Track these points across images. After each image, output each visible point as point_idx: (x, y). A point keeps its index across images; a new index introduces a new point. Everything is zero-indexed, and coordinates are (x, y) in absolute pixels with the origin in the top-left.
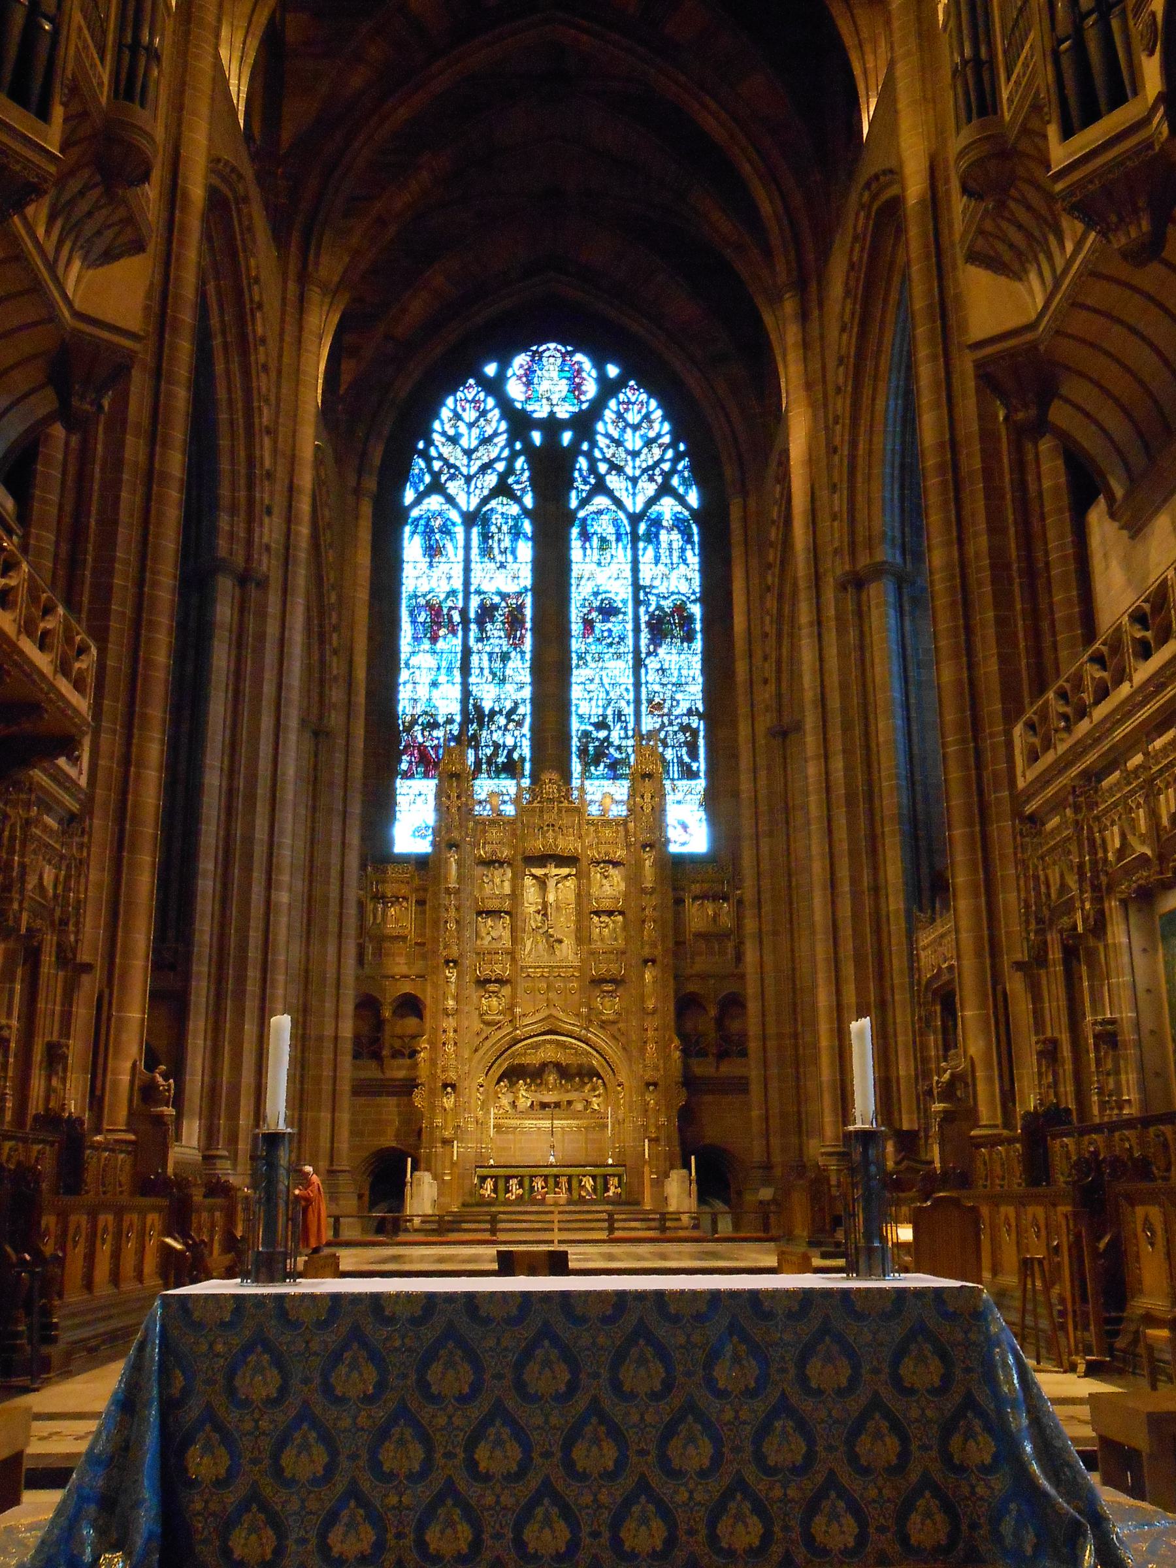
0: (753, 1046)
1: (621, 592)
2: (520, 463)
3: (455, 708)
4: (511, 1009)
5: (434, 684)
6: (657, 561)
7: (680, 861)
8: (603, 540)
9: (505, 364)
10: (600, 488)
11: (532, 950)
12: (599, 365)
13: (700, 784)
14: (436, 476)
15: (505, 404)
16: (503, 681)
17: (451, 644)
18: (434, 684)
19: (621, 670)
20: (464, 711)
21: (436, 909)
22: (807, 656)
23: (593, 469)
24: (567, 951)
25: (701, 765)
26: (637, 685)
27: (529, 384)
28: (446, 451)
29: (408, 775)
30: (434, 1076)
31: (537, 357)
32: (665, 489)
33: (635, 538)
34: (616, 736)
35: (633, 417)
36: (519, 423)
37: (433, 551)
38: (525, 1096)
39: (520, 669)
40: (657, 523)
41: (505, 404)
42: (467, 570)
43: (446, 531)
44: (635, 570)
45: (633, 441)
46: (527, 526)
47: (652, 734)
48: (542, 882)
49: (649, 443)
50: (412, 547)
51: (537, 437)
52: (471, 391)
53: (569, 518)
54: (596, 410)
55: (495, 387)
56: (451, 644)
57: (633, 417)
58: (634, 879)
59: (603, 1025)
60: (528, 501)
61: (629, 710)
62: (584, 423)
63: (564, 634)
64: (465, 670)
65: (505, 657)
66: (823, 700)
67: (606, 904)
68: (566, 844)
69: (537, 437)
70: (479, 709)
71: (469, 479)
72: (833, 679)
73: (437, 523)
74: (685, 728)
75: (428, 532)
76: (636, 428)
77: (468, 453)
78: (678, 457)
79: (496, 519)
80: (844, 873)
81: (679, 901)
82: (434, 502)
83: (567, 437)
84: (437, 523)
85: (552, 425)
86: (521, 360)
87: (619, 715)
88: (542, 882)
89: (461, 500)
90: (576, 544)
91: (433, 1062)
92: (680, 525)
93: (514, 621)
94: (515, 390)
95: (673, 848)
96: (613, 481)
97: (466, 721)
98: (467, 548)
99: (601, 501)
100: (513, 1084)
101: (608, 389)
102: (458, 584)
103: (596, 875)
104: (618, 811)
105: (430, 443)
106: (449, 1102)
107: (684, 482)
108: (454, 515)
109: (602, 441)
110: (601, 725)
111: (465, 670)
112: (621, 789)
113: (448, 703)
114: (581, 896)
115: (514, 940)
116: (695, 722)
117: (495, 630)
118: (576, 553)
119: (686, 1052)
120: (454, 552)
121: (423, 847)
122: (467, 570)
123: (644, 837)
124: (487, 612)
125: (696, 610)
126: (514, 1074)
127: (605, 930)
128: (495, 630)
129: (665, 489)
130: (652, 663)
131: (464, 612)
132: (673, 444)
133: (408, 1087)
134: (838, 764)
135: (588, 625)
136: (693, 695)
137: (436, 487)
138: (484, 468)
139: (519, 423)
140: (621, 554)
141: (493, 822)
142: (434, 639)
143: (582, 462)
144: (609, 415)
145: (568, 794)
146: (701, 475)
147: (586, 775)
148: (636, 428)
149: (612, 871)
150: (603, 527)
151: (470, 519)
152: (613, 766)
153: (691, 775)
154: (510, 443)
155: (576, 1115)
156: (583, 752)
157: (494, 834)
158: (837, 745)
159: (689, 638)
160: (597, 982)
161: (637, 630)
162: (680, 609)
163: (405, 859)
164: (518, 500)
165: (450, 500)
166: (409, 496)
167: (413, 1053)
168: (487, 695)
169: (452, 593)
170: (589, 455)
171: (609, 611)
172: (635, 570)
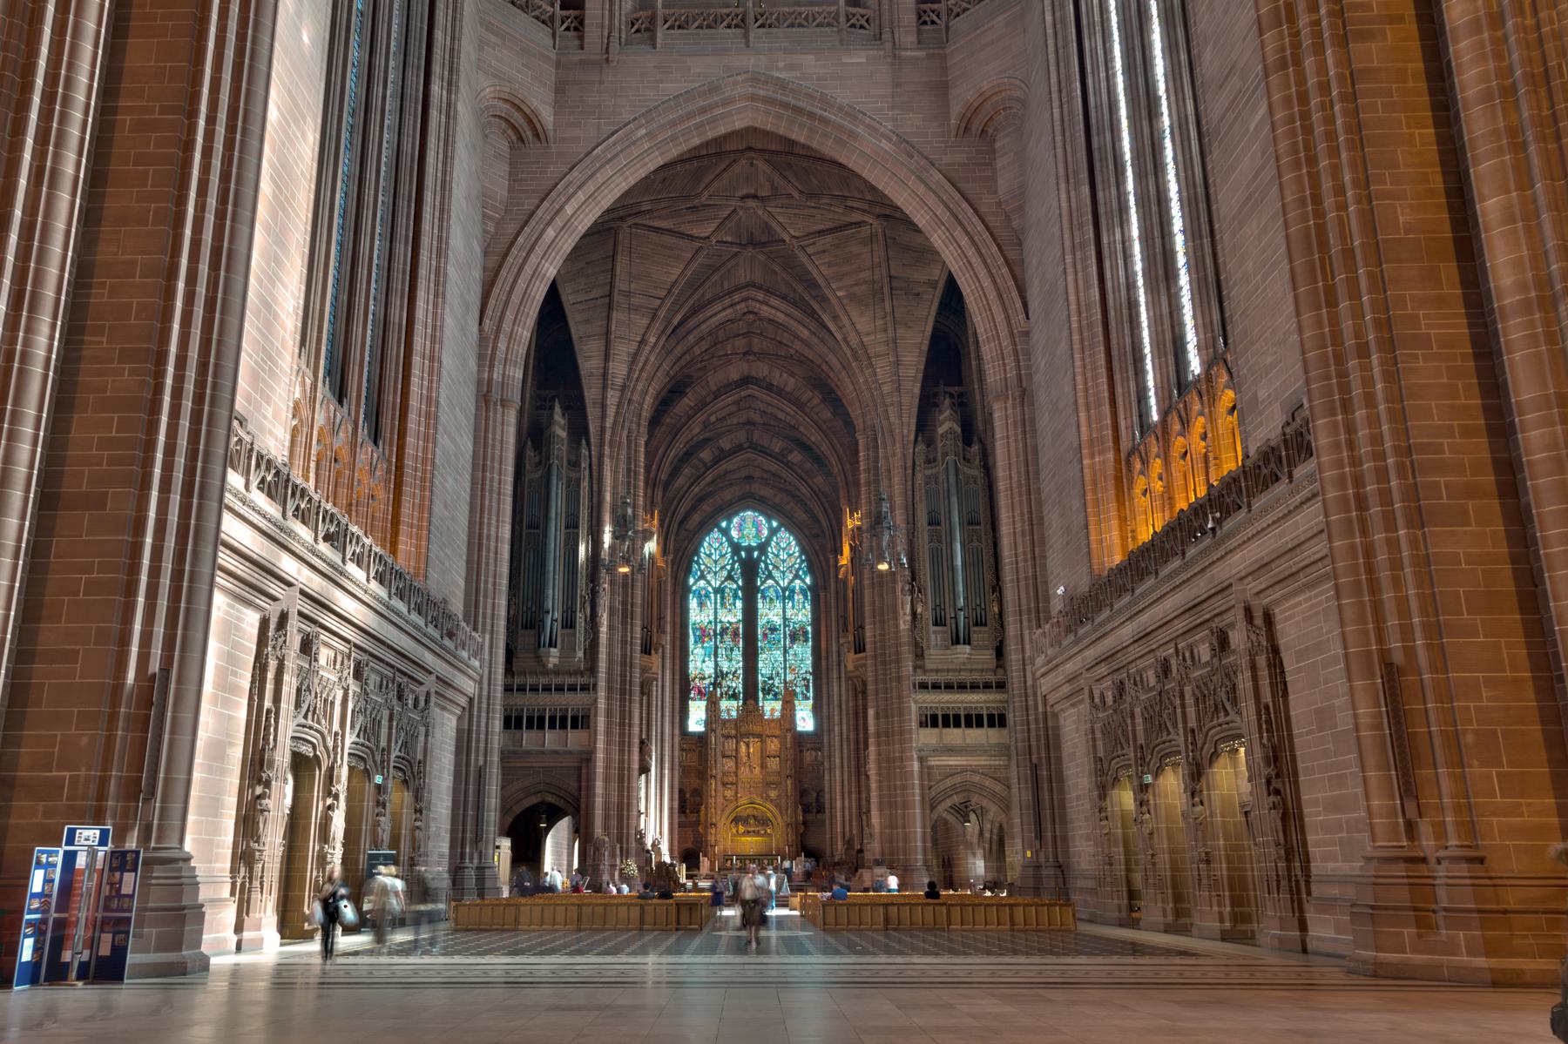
0: (827, 811)
1: (778, 621)
2: (737, 565)
3: (712, 671)
4: (736, 793)
5: (704, 661)
6: (793, 607)
7: (802, 735)
8: (771, 599)
9: (730, 522)
10: (770, 576)
11: (744, 772)
12: (769, 520)
13: (811, 702)
14: (702, 572)
15: (730, 539)
16: (731, 660)
17: (709, 644)
18: (704, 661)
19: (778, 654)
20: (716, 673)
21: (706, 755)
22: (836, 689)
23: (767, 568)
24: (757, 770)
25: (811, 694)
26: (785, 661)
27: (740, 530)
28: (706, 561)
29: (693, 699)
30: (706, 821)
31: (743, 520)
32: (797, 576)
33: (784, 598)
34: (777, 681)
35: (783, 545)
36: (736, 548)
37: (701, 605)
38: (741, 829)
39: (738, 655)
40: (793, 591)
41: (730, 539)
42: (716, 613)
43: (707, 596)
44: (784, 612)
45: (783, 556)
46: (740, 593)
47: (791, 682)
48: (748, 746)
49: (790, 556)
50: (693, 603)
51: (743, 554)
52: (716, 534)
53: (757, 589)
54: (769, 540)
55: (726, 532)
56: (709, 644)
57: (783, 545)
58: (783, 743)
59: (771, 801)
60: (740, 583)
61: (782, 671)
62: (762, 548)
63: (755, 639)
64: (716, 655)
65: (732, 650)
66: (840, 706)
67: (773, 753)
68: (757, 729)
69: (743, 554)
70: (721, 672)
71: (715, 573)
72: (844, 698)
73: (703, 592)
74: (804, 679)
75: (700, 596)
76: (784, 549)
77: (715, 562)
78: (802, 562)
79: (727, 590)
80: (845, 764)
81: (801, 751)
82: (702, 583)
83: (756, 554)
84: (703, 592)
85: (749, 549)
86: (736, 520)
87: (778, 674)
88: (748, 746)
89: (713, 583)
90: (760, 601)
91: (706, 815)
92: (803, 592)
93: (735, 634)
94: (734, 534)
95: (799, 729)
96: (776, 574)
97: (717, 677)
98: (716, 603)
99: (770, 582)
100: (737, 824)
101: (773, 532)
102: (712, 618)
103: (768, 741)
104: (777, 714)
105: (699, 557)
106: (713, 831)
107: (804, 573)
108: (710, 589)
109: (771, 556)
110: (771, 678)
111: (716, 655)
112: (778, 705)
113: (709, 669)
114: (763, 750)
115: (737, 767)
116: (810, 677)
117: (727, 638)
118: (760, 605)
119: (804, 811)
120: (710, 605)
121: (701, 729)
122: (716, 613)
123: (787, 726)
124: (724, 631)
125: (809, 628)
126: (736, 820)
127: (773, 764)
128: (727, 638)
129: (797, 576)
130: (791, 652)
131: (715, 631)
132: (800, 557)
133: (698, 823)
134: (844, 727)
135: (765, 635)
136: (808, 664)
137: (703, 577)
138: (723, 568)
139: (736, 548)
140: (778, 604)
141: (729, 720)
142: (703, 642)
143: (763, 565)
144: (773, 544)
145: (758, 710)
146: (811, 570)
147: (764, 699)
148: (784, 549)
149: (775, 740)
150: (771, 593)
151: (717, 591)
152: (776, 695)
153: (807, 698)
154: (732, 558)
155: (762, 836)
156: (763, 690)
157: (728, 725)
158: (844, 721)
159: (806, 640)
160: (768, 784)
161: (785, 638)
162: (803, 628)
163: (693, 734)
164: (736, 582)
165: (708, 582)
166: (691, 581)
167: (698, 812)
168: (725, 666)
169: (710, 622)
170: (765, 562)
171: (773, 630)
172: (784, 612)
